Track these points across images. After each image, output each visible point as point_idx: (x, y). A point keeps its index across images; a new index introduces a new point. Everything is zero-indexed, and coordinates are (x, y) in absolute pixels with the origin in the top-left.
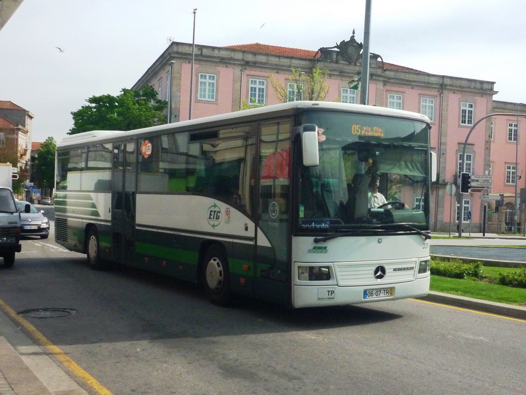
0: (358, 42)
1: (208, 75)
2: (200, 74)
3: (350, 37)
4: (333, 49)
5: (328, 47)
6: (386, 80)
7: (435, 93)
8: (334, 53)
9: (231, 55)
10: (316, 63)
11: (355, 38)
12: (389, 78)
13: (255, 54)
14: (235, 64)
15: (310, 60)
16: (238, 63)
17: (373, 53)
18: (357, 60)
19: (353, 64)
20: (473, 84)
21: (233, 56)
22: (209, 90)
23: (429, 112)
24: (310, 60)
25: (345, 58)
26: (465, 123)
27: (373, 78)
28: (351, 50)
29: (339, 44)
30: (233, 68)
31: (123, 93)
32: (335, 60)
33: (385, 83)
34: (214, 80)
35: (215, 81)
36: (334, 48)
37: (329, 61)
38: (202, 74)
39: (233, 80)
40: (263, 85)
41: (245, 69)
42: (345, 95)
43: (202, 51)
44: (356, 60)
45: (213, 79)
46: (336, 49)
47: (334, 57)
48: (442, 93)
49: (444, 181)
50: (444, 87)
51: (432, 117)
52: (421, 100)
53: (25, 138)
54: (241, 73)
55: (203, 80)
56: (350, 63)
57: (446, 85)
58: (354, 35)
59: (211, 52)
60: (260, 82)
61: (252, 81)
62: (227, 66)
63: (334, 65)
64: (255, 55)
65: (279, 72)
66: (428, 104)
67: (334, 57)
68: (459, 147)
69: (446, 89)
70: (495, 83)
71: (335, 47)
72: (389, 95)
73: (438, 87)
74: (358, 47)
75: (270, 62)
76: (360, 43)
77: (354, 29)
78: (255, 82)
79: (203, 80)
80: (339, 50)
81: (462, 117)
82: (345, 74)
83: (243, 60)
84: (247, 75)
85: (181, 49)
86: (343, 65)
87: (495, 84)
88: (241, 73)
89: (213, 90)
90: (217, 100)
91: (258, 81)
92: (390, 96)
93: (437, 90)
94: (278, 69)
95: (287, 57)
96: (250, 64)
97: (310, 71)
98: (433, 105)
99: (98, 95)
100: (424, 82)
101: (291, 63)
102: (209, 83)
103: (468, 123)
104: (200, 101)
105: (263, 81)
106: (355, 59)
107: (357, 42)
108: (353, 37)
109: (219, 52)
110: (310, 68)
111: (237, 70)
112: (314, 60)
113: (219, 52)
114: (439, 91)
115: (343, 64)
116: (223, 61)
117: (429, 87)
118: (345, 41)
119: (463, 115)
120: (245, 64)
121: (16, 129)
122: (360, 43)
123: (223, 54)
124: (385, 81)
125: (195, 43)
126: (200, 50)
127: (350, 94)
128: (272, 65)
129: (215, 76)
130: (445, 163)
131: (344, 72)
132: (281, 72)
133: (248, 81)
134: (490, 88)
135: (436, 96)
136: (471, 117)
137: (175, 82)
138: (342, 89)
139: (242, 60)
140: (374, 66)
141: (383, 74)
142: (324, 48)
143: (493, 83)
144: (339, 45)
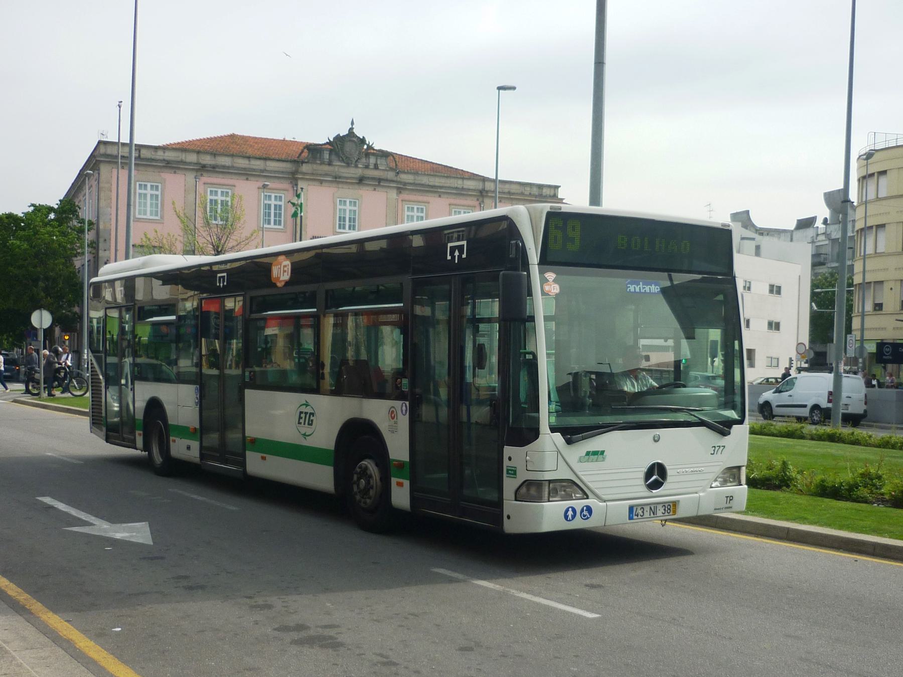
2: (138, 183)
3: (348, 129)
4: (323, 146)
8: (325, 152)
9: (181, 157)
10: (301, 165)
11: (354, 131)
12: (405, 184)
13: (214, 155)
15: (294, 162)
18: (359, 160)
19: (353, 165)
20: (528, 189)
22: (151, 204)
24: (294, 162)
25: (341, 157)
27: (382, 184)
28: (349, 147)
29: (332, 140)
31: (32, 208)
32: (328, 160)
33: (400, 190)
34: (158, 191)
35: (159, 193)
36: (325, 144)
37: (319, 162)
38: (140, 183)
39: (185, 191)
41: (202, 175)
42: (342, 207)
43: (140, 151)
44: (357, 160)
50: (485, 194)
52: (453, 212)
55: (143, 191)
56: (348, 165)
57: (487, 192)
58: (354, 127)
59: (153, 153)
61: (211, 191)
62: (175, 173)
63: (326, 168)
64: (215, 157)
67: (326, 156)
69: (487, 196)
70: (560, 186)
72: (406, 206)
73: (478, 194)
74: (360, 142)
75: (235, 165)
77: (353, 120)
78: (216, 192)
79: (143, 191)
82: (340, 180)
85: (111, 150)
86: (338, 168)
87: (559, 189)
89: (157, 204)
90: (162, 217)
91: (219, 191)
92: (408, 208)
93: (475, 199)
94: (247, 174)
95: (260, 159)
96: (207, 169)
97: (293, 178)
100: (457, 188)
101: (266, 166)
102: (152, 195)
104: (139, 220)
105: (228, 190)
106: (356, 159)
107: (357, 136)
108: (351, 129)
109: (164, 152)
110: (291, 173)
111: (190, 177)
113: (164, 152)
114: (478, 200)
115: (339, 165)
116: (170, 165)
117: (463, 195)
120: (199, 169)
122: (362, 138)
123: (170, 155)
126: (138, 151)
127: (350, 206)
128: (238, 169)
129: (160, 185)
131: (340, 177)
132: (252, 178)
133: (206, 192)
134: (552, 194)
137: (102, 195)
138: (338, 200)
139: (196, 164)
140: (384, 168)
141: (395, 179)
143: (557, 187)
144: (332, 140)
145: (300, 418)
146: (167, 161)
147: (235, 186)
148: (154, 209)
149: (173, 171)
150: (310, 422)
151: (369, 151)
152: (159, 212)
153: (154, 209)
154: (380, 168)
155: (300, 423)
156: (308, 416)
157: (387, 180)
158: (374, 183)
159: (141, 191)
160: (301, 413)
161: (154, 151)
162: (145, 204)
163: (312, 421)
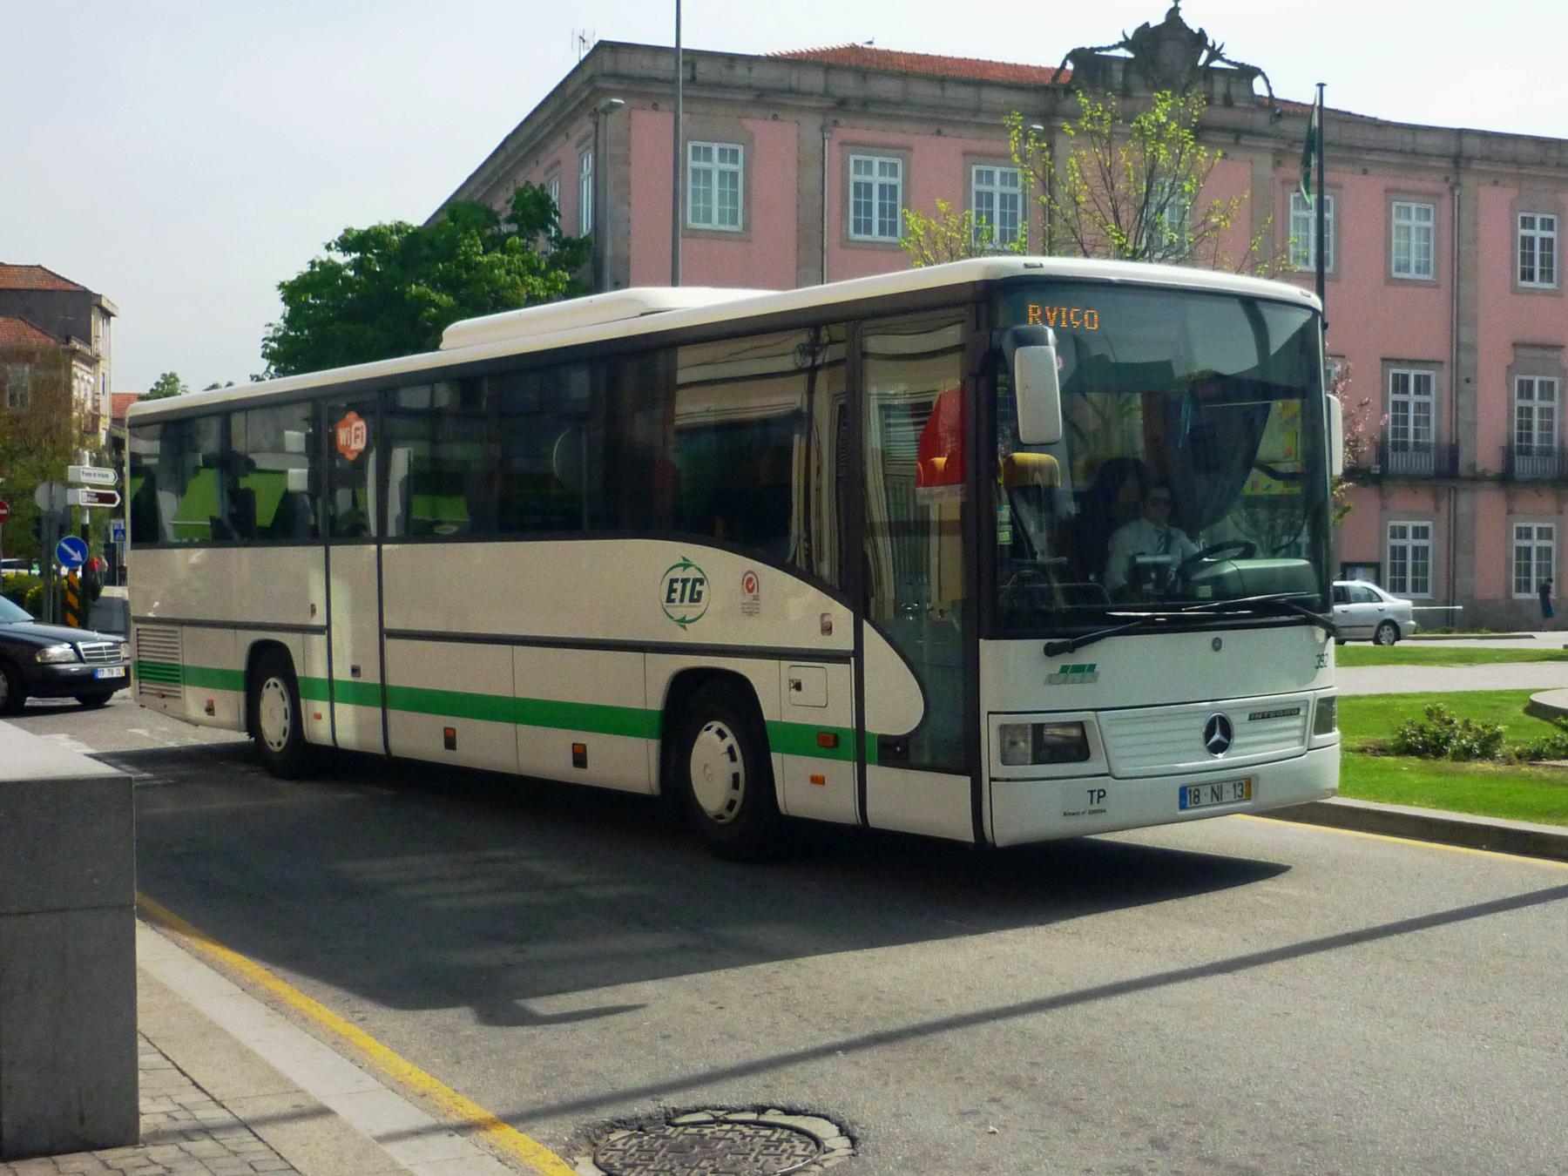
0: (1190, 26)
1: (715, 148)
5: (1095, 46)
6: (1282, 146)
7: (1432, 182)
11: (1181, 14)
14: (801, 109)
16: (814, 104)
17: (1240, 61)
21: (794, 83)
22: (722, 195)
23: (1418, 247)
26: (1531, 278)
27: (1243, 142)
28: (1170, 53)
29: (1130, 37)
30: (796, 122)
35: (739, 167)
36: (1115, 47)
40: (894, 173)
43: (693, 67)
45: (734, 160)
46: (1122, 53)
47: (1118, 77)
48: (1458, 184)
49: (1473, 466)
51: (1428, 262)
53: (92, 380)
54: (824, 139)
57: (1470, 159)
60: (882, 164)
62: (775, 117)
65: (945, 130)
66: (1414, 222)
67: (1118, 77)
68: (1516, 356)
71: (1120, 45)
76: (1196, 31)
80: (1130, 55)
81: (1523, 262)
83: (826, 94)
84: (843, 144)
85: (626, 65)
88: (824, 139)
91: (876, 161)
98: (1430, 224)
99: (362, 224)
102: (722, 174)
103: (1542, 280)
104: (695, 233)
105: (894, 160)
107: (1187, 28)
109: (750, 69)
111: (811, 127)
112: (1054, 90)
113: (750, 69)
114: (1447, 179)
118: (1152, 25)
119: (1523, 255)
121: (65, 351)
122: (1196, 31)
124: (1280, 150)
125: (684, 45)
130: (1474, 408)
133: (845, 167)
135: (1439, 196)
136: (1551, 257)
140: (1245, 105)
141: (1270, 130)
142: (1083, 49)
144: (1130, 37)
145: (671, 590)
146: (757, 89)
147: (910, 149)
148: (728, 207)
149: (772, 112)
150: (695, 597)
151: (1217, 64)
152: (740, 216)
153: (728, 207)
154: (1236, 104)
155: (670, 600)
156: (689, 585)
157: (1251, 133)
158: (1226, 140)
159: (697, 164)
160: (673, 581)
161: (726, 67)
162: (708, 197)
163: (700, 593)
